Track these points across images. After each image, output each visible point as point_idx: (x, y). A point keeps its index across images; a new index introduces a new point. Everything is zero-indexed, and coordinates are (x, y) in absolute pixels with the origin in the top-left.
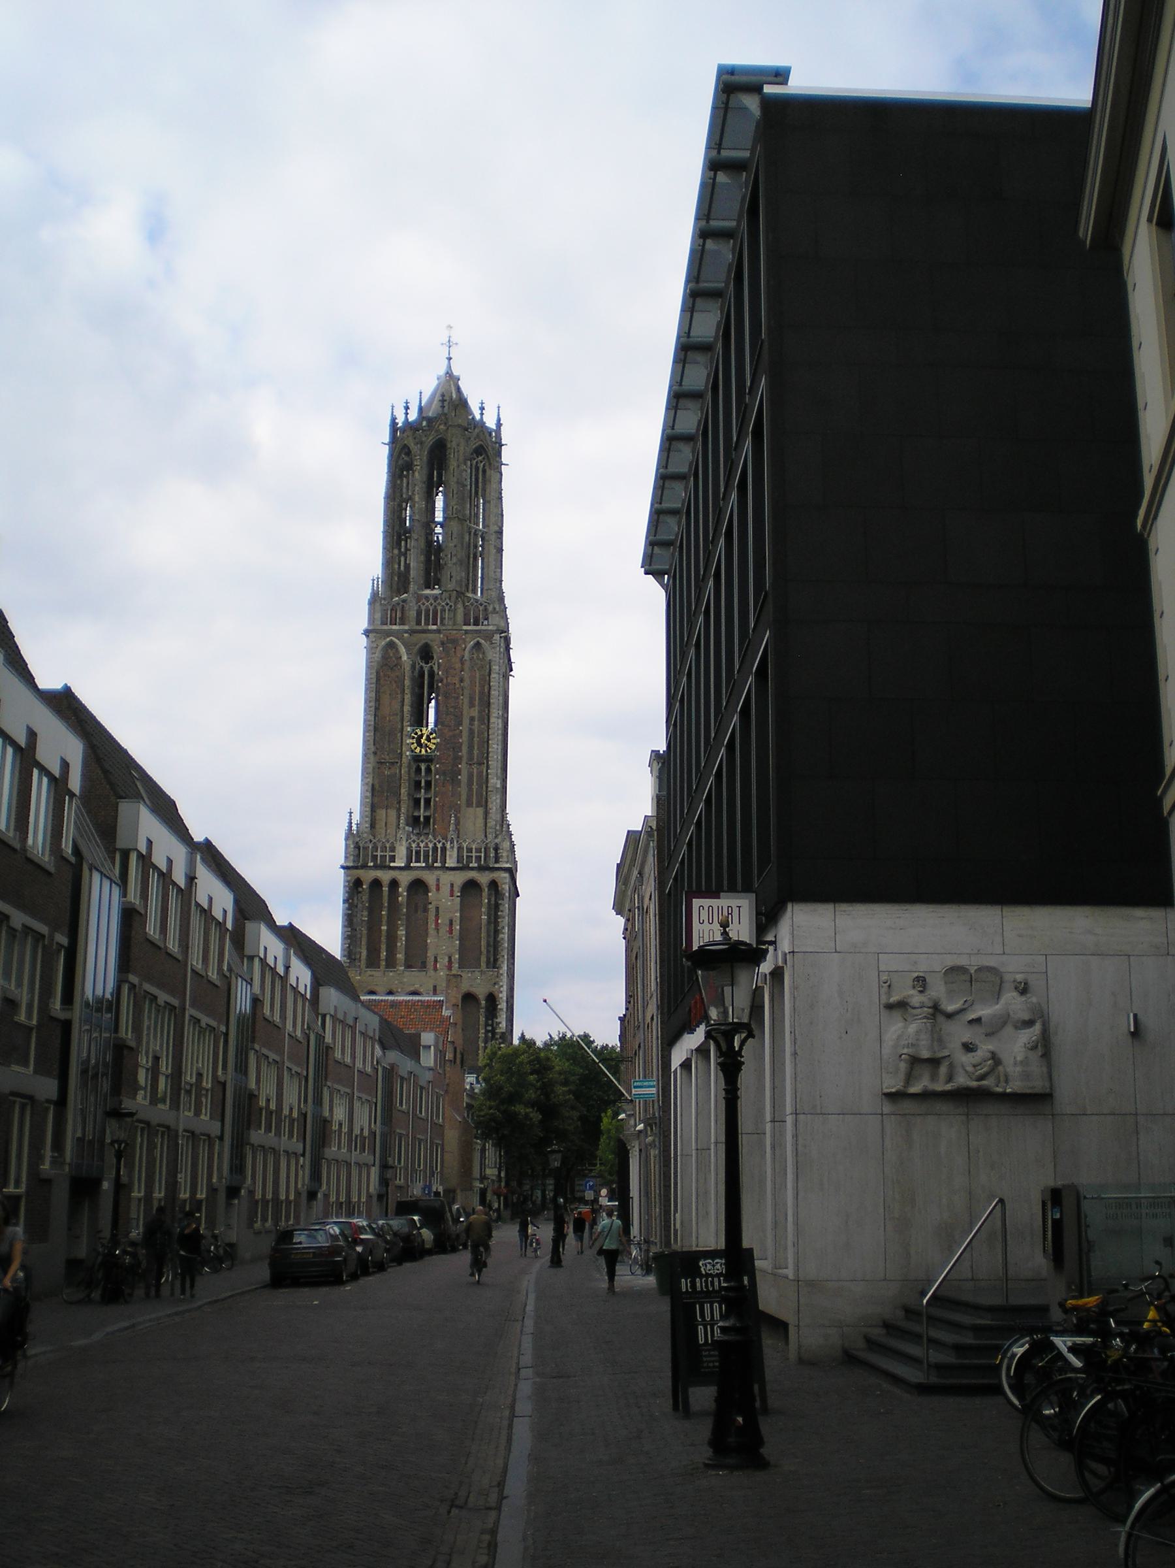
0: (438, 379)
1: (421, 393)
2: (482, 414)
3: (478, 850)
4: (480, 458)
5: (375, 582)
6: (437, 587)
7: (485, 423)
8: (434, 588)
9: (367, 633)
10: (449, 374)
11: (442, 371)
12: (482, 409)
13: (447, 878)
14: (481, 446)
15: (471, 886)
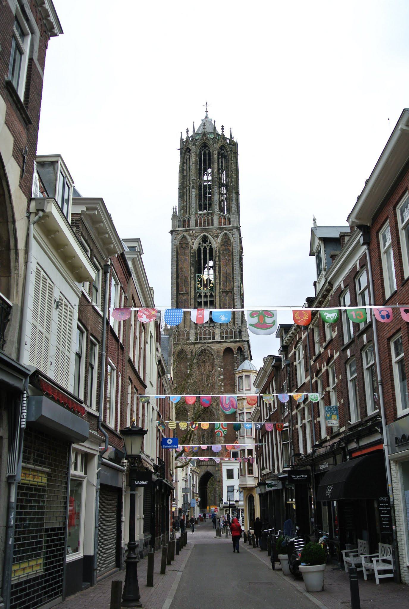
0: (202, 120)
1: (194, 123)
2: (223, 131)
3: (231, 332)
4: (223, 152)
5: (175, 209)
6: (205, 210)
7: (224, 135)
8: (204, 211)
9: (171, 232)
10: (206, 117)
11: (204, 118)
12: (223, 129)
13: (216, 347)
14: (223, 145)
15: (228, 350)
